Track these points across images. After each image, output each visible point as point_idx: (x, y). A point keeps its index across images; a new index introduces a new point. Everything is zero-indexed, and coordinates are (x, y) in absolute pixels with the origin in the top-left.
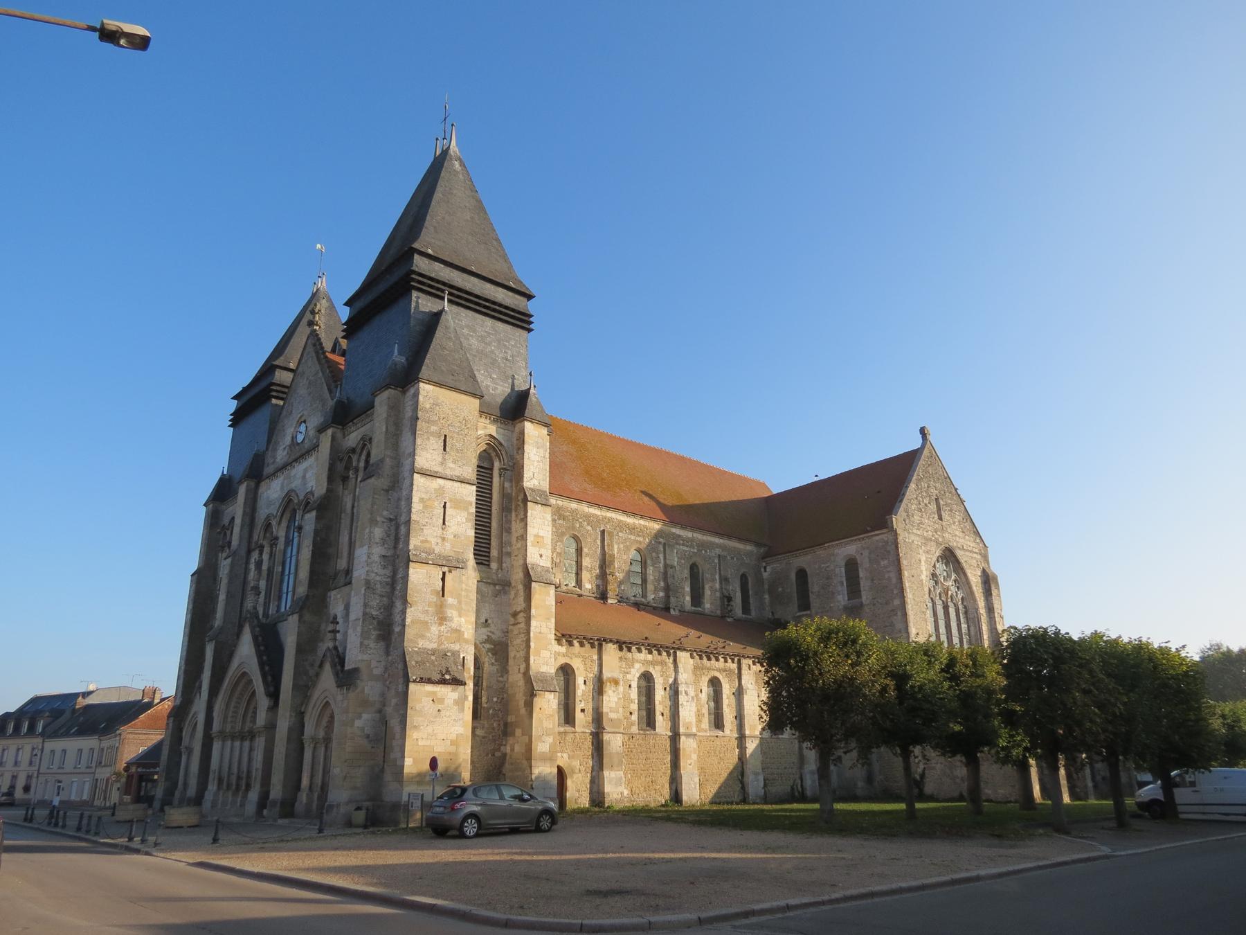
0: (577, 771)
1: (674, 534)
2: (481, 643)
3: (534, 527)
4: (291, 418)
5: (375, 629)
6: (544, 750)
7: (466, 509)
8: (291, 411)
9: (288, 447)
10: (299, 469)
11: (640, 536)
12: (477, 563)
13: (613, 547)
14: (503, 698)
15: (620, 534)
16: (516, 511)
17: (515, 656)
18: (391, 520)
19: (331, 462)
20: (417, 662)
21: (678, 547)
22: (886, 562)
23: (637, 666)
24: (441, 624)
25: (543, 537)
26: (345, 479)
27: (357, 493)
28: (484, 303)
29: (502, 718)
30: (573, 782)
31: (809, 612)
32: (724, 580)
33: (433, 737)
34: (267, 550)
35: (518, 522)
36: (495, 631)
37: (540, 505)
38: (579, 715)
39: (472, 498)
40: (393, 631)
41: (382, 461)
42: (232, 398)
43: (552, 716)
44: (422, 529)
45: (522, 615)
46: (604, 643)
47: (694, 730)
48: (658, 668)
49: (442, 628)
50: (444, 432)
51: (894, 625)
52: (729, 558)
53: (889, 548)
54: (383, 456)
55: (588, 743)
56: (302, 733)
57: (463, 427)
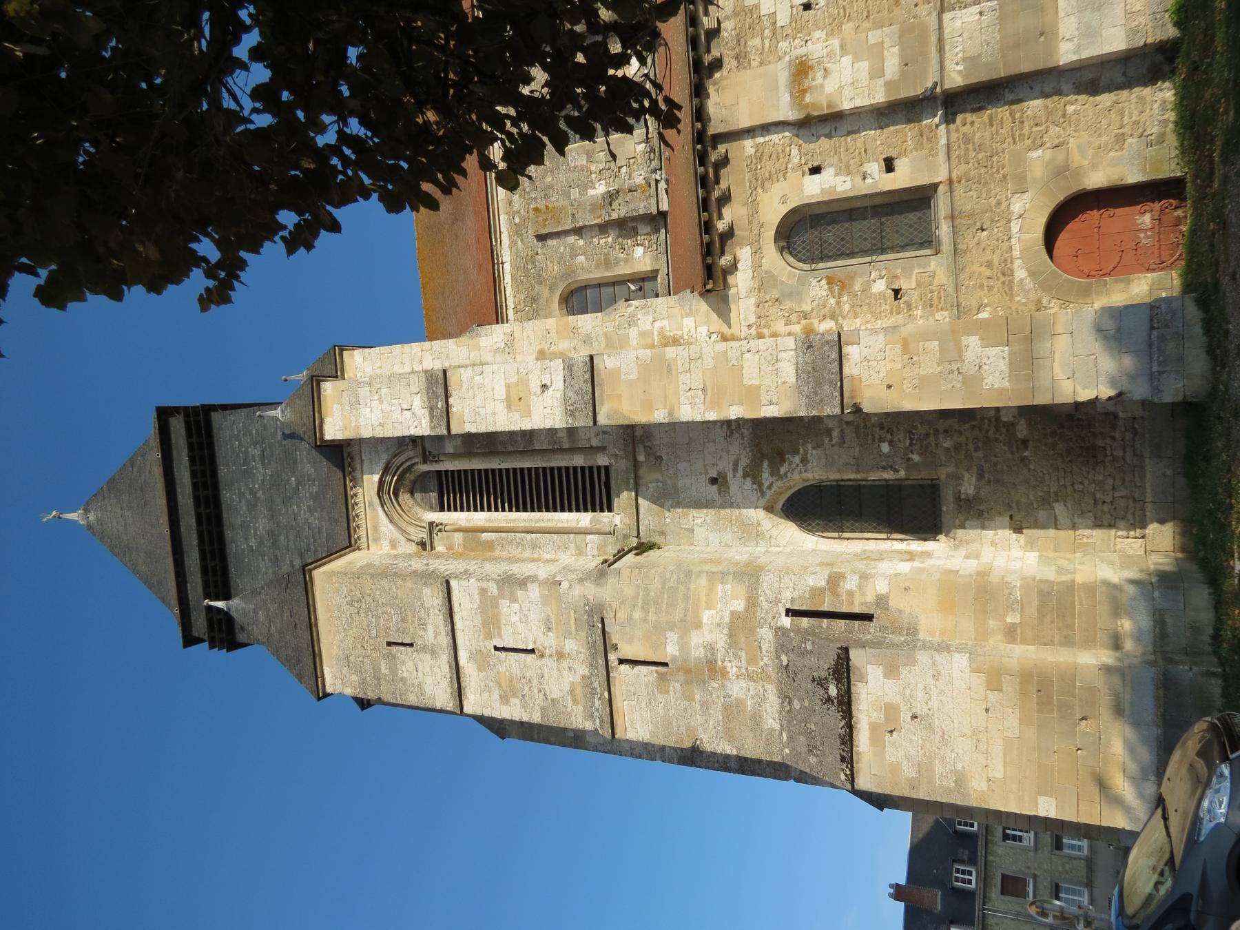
0: (1060, 156)
2: (763, 494)
3: (494, 414)
6: (1003, 366)
24: (724, 674)
25: (508, 387)
30: (1094, 166)
33: (983, 737)
36: (733, 458)
37: (451, 400)
38: (904, 177)
44: (553, 700)
46: (713, 129)
49: (731, 667)
55: (971, 124)
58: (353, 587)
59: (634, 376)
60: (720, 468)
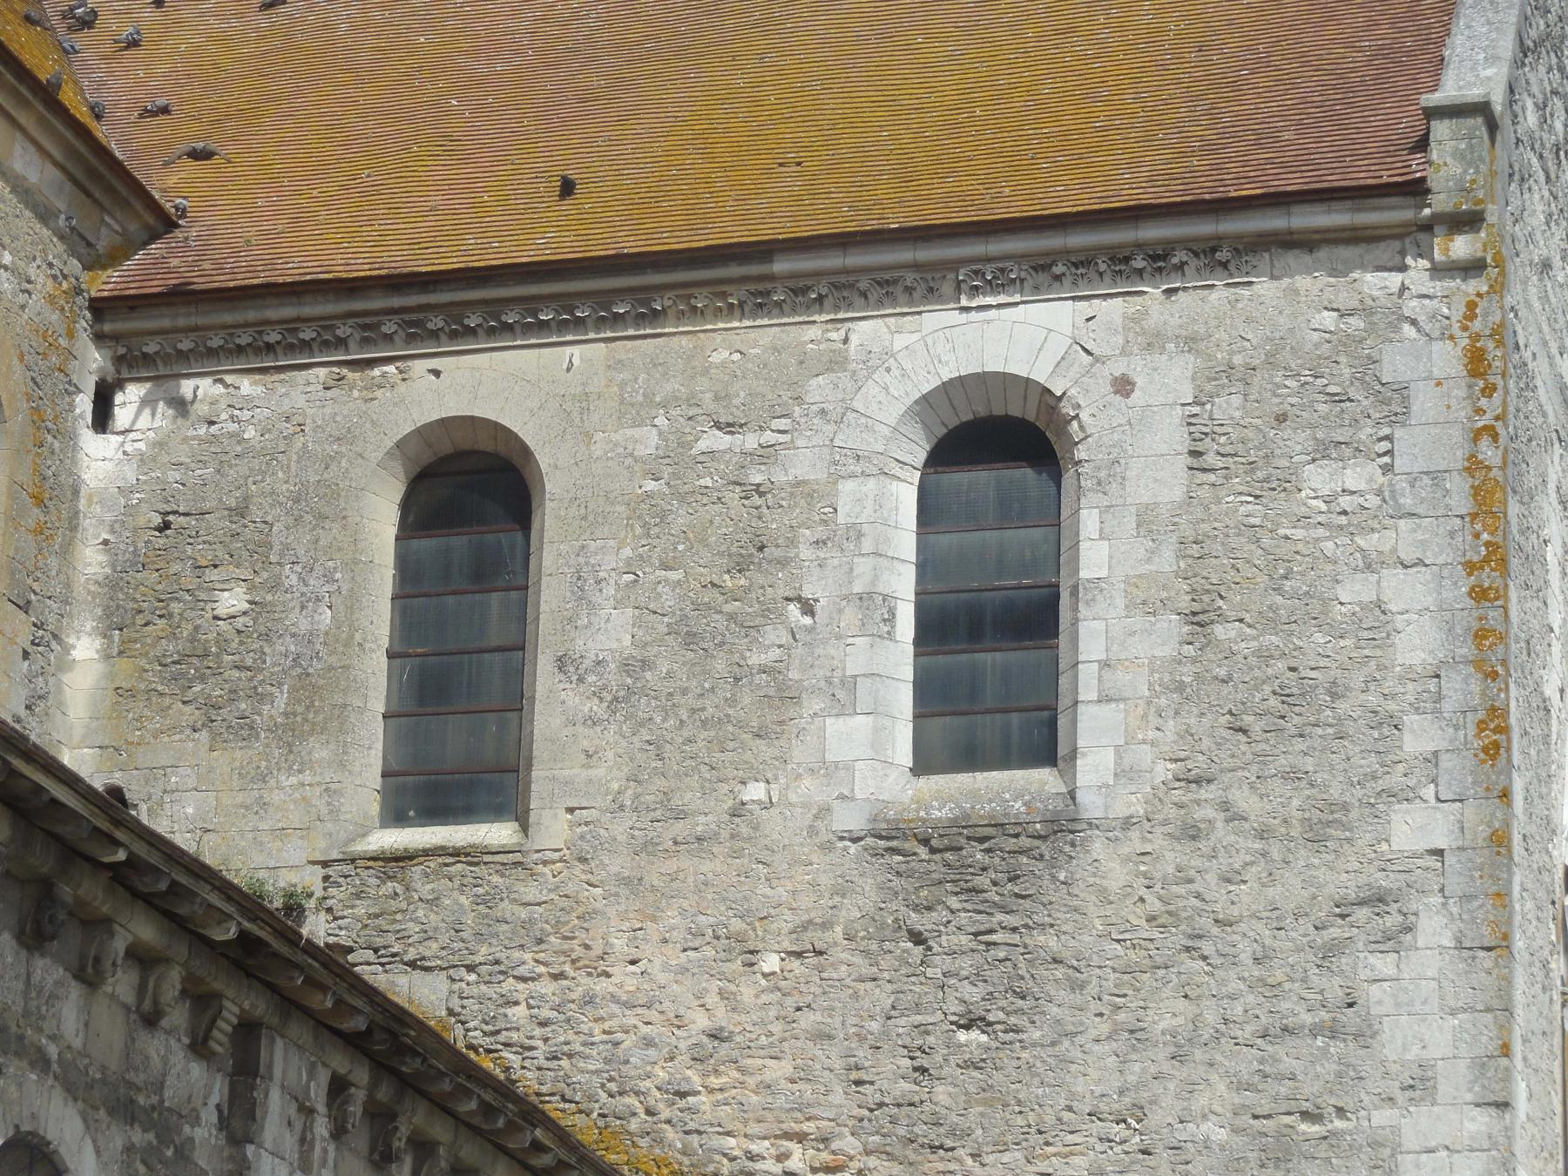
22: (1358, 476)
31: (498, 833)
51: (1365, 1035)
53: (1395, 364)
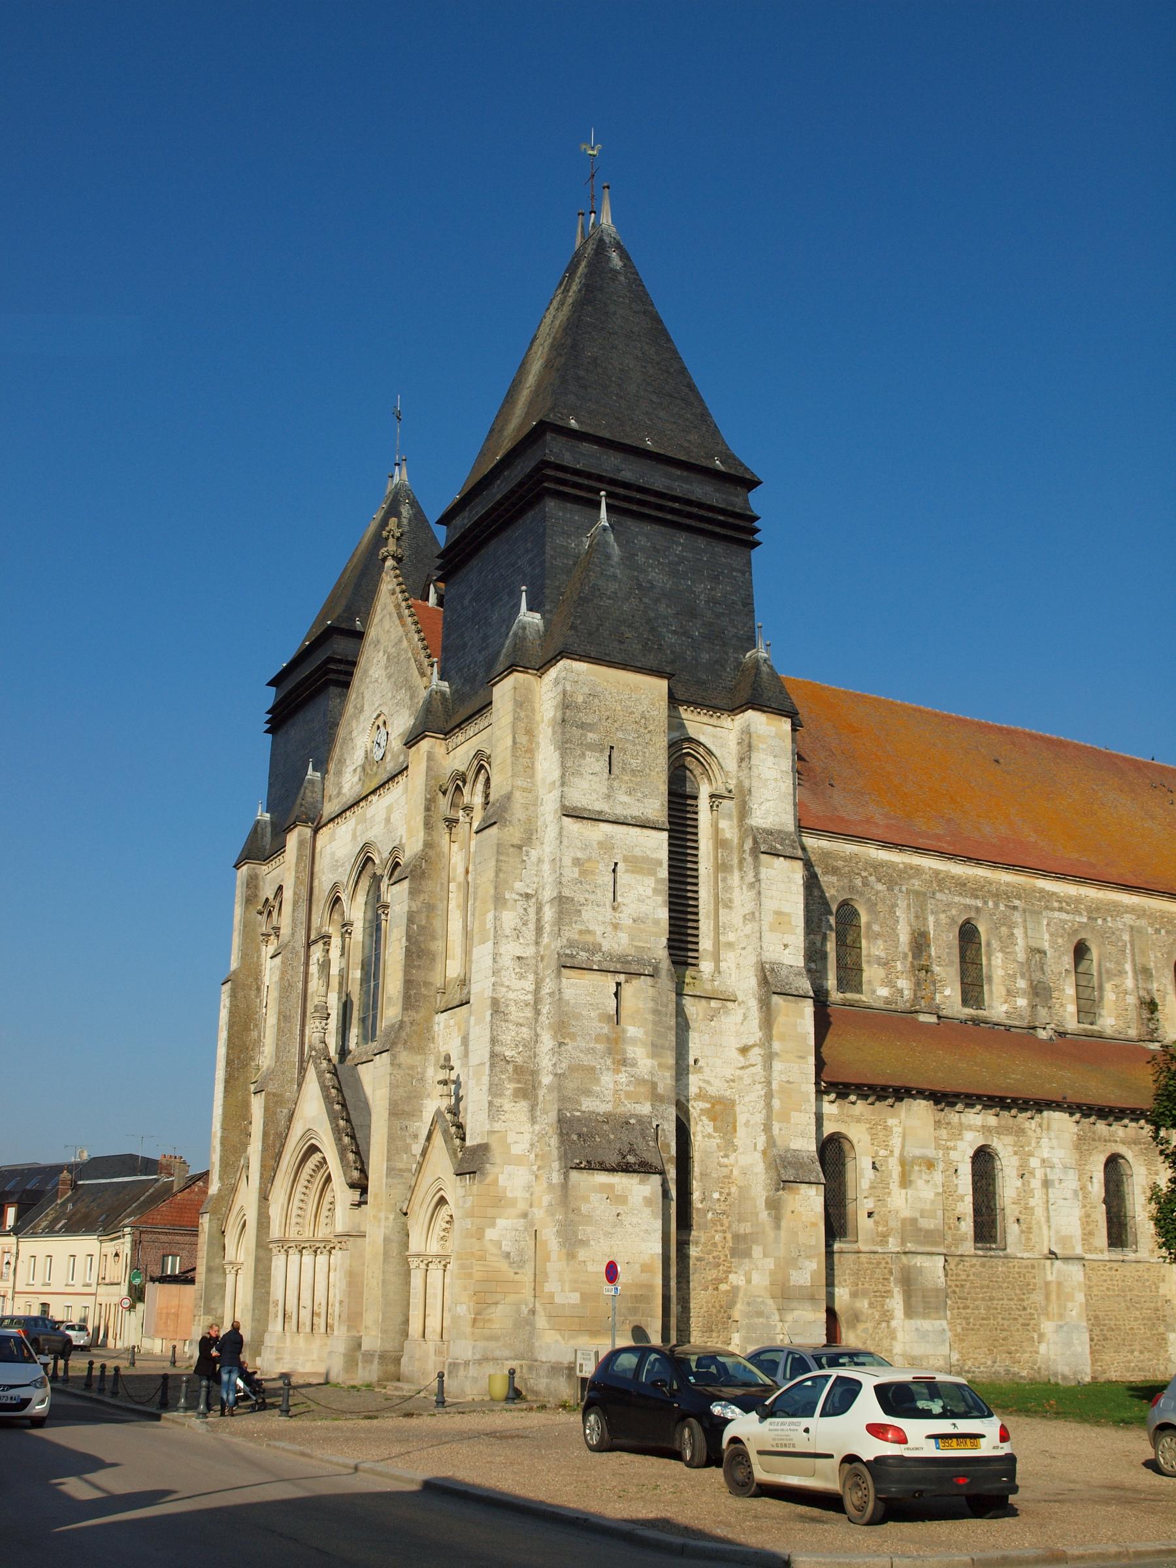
1: (1042, 890)
4: (362, 718)
5: (510, 1080)
6: (801, 1282)
7: (651, 872)
8: (362, 706)
9: (359, 770)
10: (378, 805)
11: (977, 897)
12: (673, 962)
13: (925, 919)
14: (729, 1194)
15: (938, 895)
16: (741, 869)
17: (748, 1121)
18: (528, 896)
19: (428, 796)
20: (579, 1136)
21: (1050, 914)
23: (969, 1136)
25: (788, 915)
26: (451, 823)
27: (472, 850)
28: (670, 504)
29: (729, 1227)
30: (857, 1336)
32: (1144, 973)
34: (336, 942)
35: (745, 887)
36: (712, 1080)
37: (782, 859)
39: (663, 855)
40: (540, 1082)
41: (508, 797)
42: (270, 684)
43: (814, 1225)
44: (580, 911)
45: (756, 1051)
47: (1079, 1250)
48: (1009, 1139)
49: (623, 1078)
50: (608, 742)
52: (1150, 930)
54: (509, 788)
56: (406, 1245)
57: (642, 730)
58: (656, 723)
59: (799, 1030)
60: (705, 1069)
